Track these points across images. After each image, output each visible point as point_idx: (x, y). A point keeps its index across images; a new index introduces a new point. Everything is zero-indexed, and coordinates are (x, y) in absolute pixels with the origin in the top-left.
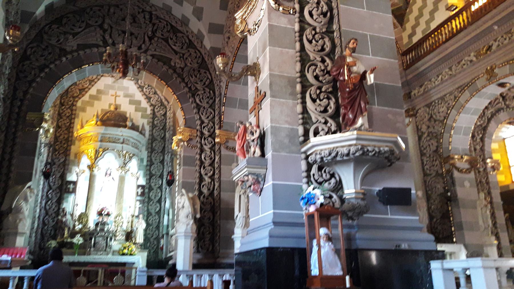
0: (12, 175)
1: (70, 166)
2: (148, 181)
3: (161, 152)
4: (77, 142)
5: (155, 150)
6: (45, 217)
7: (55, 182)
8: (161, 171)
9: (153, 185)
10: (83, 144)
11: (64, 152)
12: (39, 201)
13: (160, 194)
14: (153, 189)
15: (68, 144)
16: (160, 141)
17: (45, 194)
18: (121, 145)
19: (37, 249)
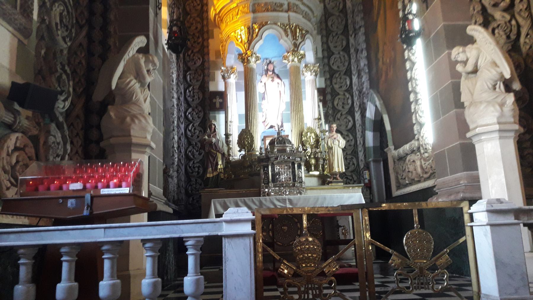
0: (111, 42)
1: (211, 71)
2: (328, 83)
3: (342, 34)
4: (216, 31)
5: (333, 31)
6: (188, 148)
7: (194, 96)
8: (346, 64)
9: (336, 87)
10: (226, 25)
11: (199, 50)
12: (176, 122)
13: (350, 101)
14: (338, 94)
15: (203, 38)
16: (339, 16)
17: (183, 115)
18: (286, 15)
19: (184, 197)
